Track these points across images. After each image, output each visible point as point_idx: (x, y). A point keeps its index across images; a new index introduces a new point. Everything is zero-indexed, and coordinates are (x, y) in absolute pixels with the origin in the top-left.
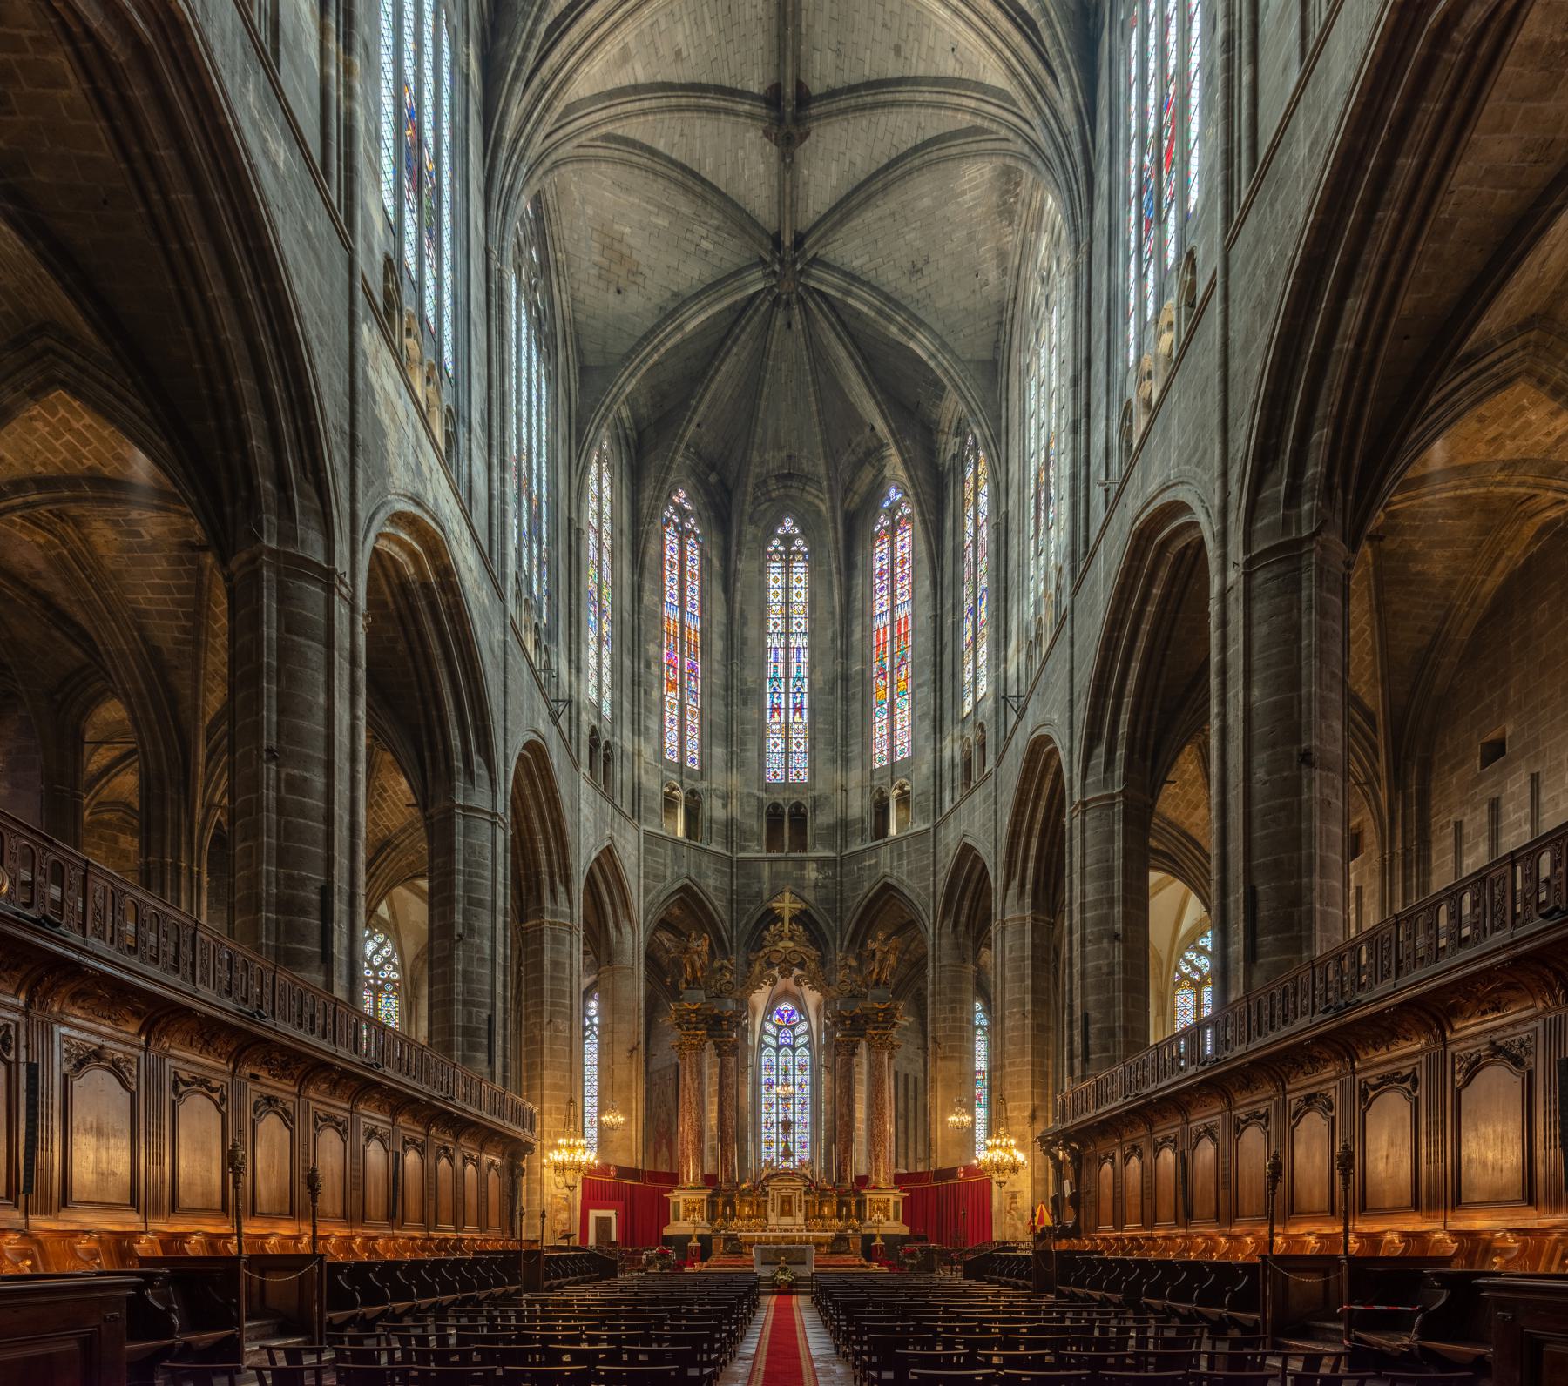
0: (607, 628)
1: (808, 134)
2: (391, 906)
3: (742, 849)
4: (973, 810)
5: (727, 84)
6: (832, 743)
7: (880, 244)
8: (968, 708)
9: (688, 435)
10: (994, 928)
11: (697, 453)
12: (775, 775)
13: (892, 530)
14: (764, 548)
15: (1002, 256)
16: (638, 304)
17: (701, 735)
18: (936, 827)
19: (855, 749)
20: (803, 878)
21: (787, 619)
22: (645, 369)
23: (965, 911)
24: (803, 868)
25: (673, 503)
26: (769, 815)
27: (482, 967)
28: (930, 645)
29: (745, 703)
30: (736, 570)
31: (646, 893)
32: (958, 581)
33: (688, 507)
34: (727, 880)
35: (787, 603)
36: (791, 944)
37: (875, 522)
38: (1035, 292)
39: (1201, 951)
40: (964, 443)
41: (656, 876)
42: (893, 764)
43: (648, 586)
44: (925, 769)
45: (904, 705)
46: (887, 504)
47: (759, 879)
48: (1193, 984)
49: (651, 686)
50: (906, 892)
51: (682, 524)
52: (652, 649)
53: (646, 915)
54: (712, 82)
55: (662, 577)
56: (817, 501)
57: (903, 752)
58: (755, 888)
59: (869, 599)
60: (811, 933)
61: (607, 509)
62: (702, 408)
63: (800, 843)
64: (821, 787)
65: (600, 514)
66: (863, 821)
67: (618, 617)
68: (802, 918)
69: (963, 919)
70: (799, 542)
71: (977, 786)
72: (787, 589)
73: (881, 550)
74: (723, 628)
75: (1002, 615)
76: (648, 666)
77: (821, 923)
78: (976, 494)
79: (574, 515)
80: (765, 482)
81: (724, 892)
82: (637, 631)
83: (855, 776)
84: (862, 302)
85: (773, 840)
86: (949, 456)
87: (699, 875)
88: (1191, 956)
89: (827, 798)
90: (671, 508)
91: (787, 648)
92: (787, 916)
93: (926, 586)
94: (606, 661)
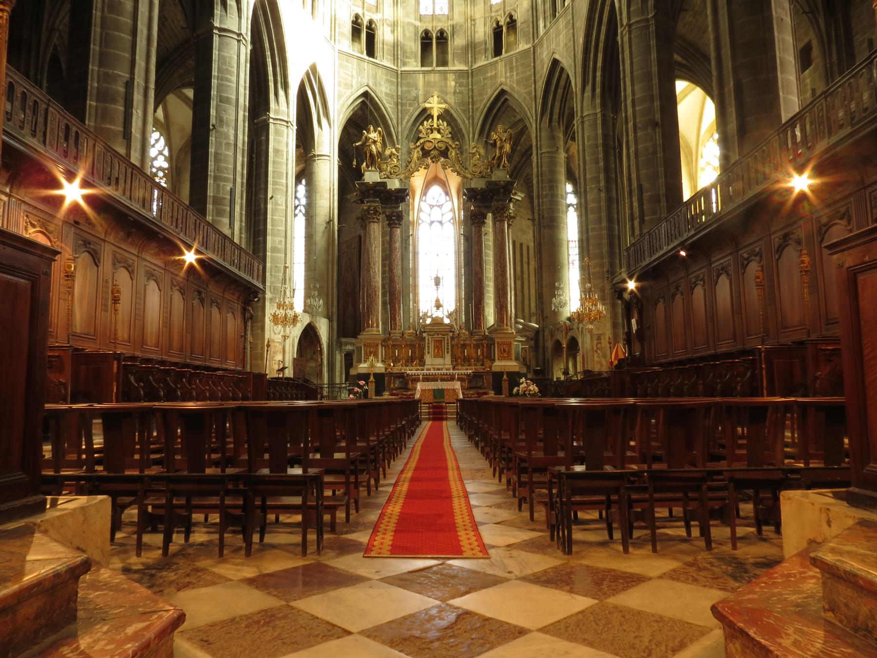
2: (165, 110)
3: (404, 64)
4: (558, 34)
10: (576, 122)
18: (534, 47)
20: (446, 86)
23: (556, 110)
24: (446, 79)
26: (422, 39)
27: (228, 150)
31: (340, 96)
34: (394, 88)
36: (439, 136)
41: (346, 85)
50: (516, 96)
53: (339, 114)
58: (414, 94)
60: (452, 128)
63: (443, 62)
64: (458, 18)
66: (486, 44)
68: (445, 115)
69: (555, 117)
71: (561, 16)
77: (459, 121)
81: (392, 96)
83: (479, 12)
87: (375, 84)
89: (461, 26)
92: (435, 114)
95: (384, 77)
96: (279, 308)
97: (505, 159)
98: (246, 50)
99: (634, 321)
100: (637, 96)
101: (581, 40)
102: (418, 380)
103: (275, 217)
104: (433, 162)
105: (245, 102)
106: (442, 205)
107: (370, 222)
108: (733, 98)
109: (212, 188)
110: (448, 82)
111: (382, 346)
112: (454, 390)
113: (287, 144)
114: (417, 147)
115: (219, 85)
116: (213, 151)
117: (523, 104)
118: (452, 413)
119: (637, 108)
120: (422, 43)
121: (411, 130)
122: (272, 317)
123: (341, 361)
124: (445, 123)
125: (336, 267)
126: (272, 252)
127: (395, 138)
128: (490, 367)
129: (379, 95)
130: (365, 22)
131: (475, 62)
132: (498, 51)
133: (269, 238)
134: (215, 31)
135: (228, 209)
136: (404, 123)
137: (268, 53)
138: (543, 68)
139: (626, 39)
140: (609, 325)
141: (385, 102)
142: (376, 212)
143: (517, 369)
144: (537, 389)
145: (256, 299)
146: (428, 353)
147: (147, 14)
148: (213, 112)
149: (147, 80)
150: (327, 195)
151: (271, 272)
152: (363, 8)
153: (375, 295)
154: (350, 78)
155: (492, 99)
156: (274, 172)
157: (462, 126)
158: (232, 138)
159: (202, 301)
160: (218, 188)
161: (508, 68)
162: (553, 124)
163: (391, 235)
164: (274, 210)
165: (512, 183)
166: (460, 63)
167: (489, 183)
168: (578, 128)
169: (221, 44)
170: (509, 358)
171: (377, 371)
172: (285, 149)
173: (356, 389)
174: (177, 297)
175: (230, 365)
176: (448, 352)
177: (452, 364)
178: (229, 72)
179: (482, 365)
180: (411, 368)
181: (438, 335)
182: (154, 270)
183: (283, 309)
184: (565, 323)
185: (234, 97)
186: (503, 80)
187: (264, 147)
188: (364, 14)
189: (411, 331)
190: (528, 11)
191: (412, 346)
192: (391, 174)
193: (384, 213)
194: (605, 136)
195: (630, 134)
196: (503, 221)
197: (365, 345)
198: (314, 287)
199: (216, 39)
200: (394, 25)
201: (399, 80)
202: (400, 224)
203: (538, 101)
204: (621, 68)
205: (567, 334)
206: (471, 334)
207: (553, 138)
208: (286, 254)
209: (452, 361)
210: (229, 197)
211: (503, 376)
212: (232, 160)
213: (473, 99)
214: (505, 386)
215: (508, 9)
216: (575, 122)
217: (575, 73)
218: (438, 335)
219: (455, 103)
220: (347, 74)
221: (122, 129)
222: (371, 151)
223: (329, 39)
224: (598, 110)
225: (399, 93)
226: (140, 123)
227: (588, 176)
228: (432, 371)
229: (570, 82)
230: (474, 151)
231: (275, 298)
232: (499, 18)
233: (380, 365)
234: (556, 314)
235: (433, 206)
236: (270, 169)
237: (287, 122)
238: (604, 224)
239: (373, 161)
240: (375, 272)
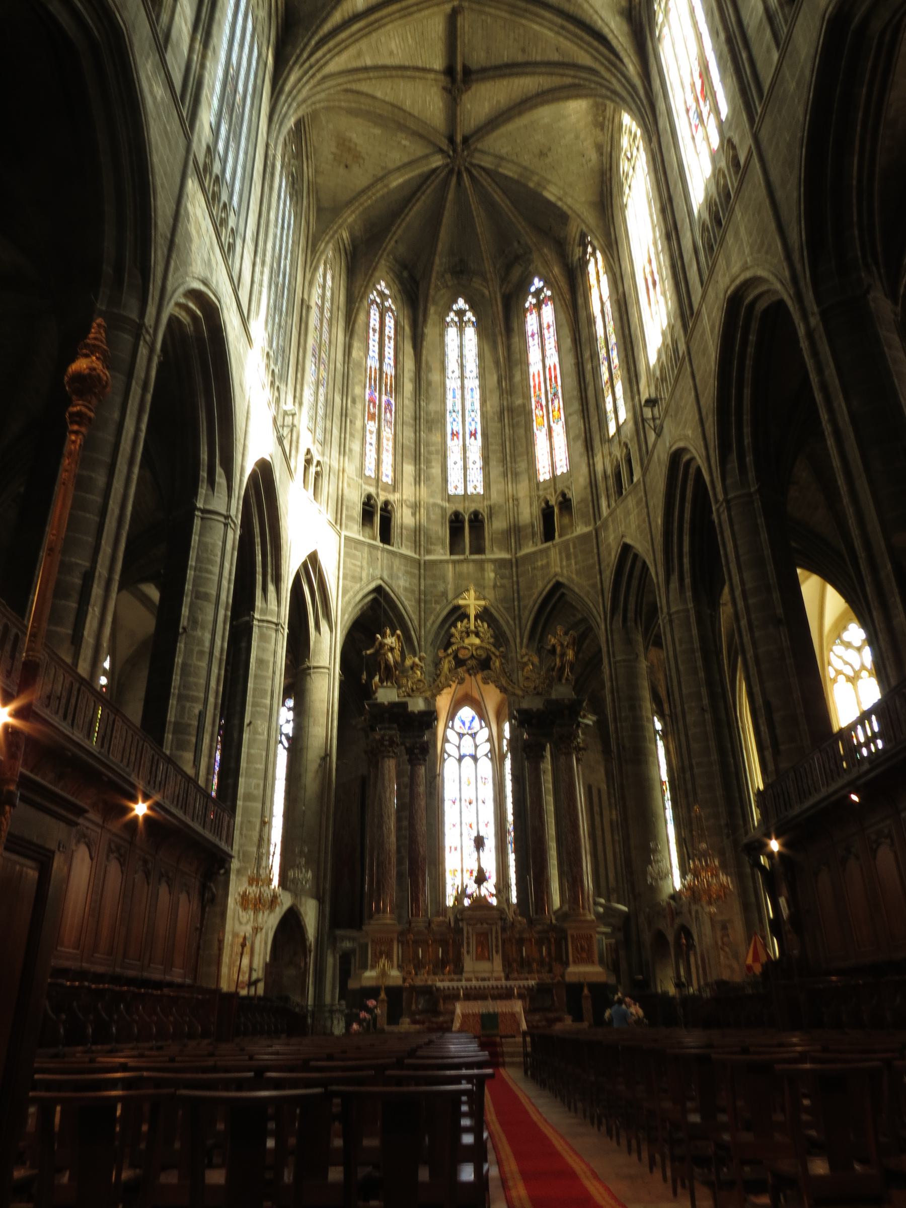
0: (323, 374)
1: (470, 88)
3: (428, 552)
5: (420, 64)
6: (503, 461)
7: (518, 141)
8: (612, 430)
9: (389, 247)
11: (396, 260)
12: (456, 487)
13: (538, 306)
14: (443, 320)
15: (599, 148)
16: (360, 178)
17: (395, 455)
19: (522, 466)
20: (484, 579)
21: (462, 367)
22: (361, 208)
24: (482, 569)
25: (377, 290)
26: (451, 522)
28: (575, 384)
29: (430, 430)
30: (423, 335)
31: (344, 594)
32: (593, 338)
33: (387, 292)
34: (416, 581)
35: (461, 356)
37: (525, 300)
38: (624, 166)
39: (848, 645)
40: (585, 252)
41: (353, 577)
42: (554, 477)
43: (356, 344)
44: (582, 479)
45: (559, 430)
46: (533, 289)
47: (444, 578)
48: (849, 679)
49: (355, 417)
50: (576, 590)
51: (383, 303)
52: (358, 390)
53: (343, 614)
54: (411, 64)
55: (368, 338)
56: (481, 288)
57: (562, 467)
58: (441, 588)
59: (525, 351)
61: (328, 294)
62: (400, 232)
63: (478, 549)
64: (496, 497)
65: (323, 297)
66: (533, 526)
67: (332, 366)
69: (631, 615)
70: (469, 315)
72: (461, 347)
73: (531, 322)
74: (412, 374)
75: (631, 361)
76: (354, 402)
78: (599, 281)
79: (306, 297)
80: (443, 276)
81: (413, 592)
82: (346, 377)
83: (523, 489)
84: (508, 171)
85: (455, 545)
86: (577, 257)
87: (391, 576)
88: (838, 649)
89: (500, 507)
90: (375, 293)
91: (463, 387)
93: (568, 342)
94: (322, 398)
95: (402, 568)
96: (251, 884)
97: (567, 670)
98: (233, 536)
99: (782, 901)
100: (749, 586)
101: (660, 521)
102: (456, 997)
103: (252, 751)
104: (470, 675)
105: (227, 597)
106: (475, 734)
107: (383, 757)
108: (894, 584)
109: (174, 711)
110: (486, 574)
111: (398, 941)
112: (513, 1015)
113: (275, 653)
114: (448, 655)
115: (196, 578)
116: (180, 661)
117: (586, 599)
118: (512, 1055)
119: (751, 601)
120: (451, 528)
121: (437, 634)
122: (239, 899)
123: (335, 965)
124: (486, 625)
125: (331, 822)
126: (245, 800)
127: (416, 643)
128: (563, 976)
129: (396, 589)
130: (379, 504)
131: (520, 549)
132: (549, 535)
133: (242, 780)
134: (198, 513)
135: (194, 739)
136: (429, 624)
137: (258, 540)
138: (610, 554)
139: (725, 516)
140: (736, 906)
141: (403, 599)
142: (392, 743)
143: (603, 978)
144: (641, 1012)
145: (222, 871)
146: (468, 952)
147: (122, 490)
148: (185, 611)
149: (111, 570)
150: (323, 721)
151: (241, 829)
152: (377, 487)
153: (390, 863)
154: (359, 570)
155: (544, 593)
156: (255, 690)
157: (505, 628)
158: (207, 644)
159: (147, 874)
160: (182, 711)
161: (564, 556)
162: (629, 624)
163: (413, 777)
164: (252, 742)
165: (580, 702)
166: (501, 550)
167: (549, 702)
168: (664, 627)
169: (203, 528)
170: (589, 961)
171: (391, 983)
172: (272, 659)
173: (363, 1014)
174: (114, 868)
175: (177, 975)
176: (497, 952)
177: (504, 971)
178: (211, 562)
179: (550, 971)
180: (442, 977)
181: (482, 924)
182: (87, 828)
183: (257, 885)
184: (669, 904)
185: (214, 592)
186: (558, 570)
187: (243, 657)
188: (378, 495)
189: (441, 918)
190: (585, 488)
191: (443, 943)
192: (413, 690)
193: (403, 744)
194: (703, 638)
195: (744, 633)
196: (569, 755)
197: (373, 941)
198: (301, 852)
199: (197, 523)
200: (416, 507)
201: (422, 571)
202: (425, 760)
203: (606, 594)
204: (722, 552)
205: (673, 920)
206: (531, 922)
207: (629, 642)
208: (264, 803)
209: (504, 966)
210: (195, 723)
211: (582, 990)
212: (204, 673)
213: (518, 593)
214: (587, 1005)
215: (560, 487)
216: (660, 621)
217: (655, 560)
218: (482, 924)
219: (496, 599)
220: (355, 565)
221: (70, 632)
222: (387, 661)
223: (334, 523)
224: (691, 605)
225: (422, 588)
226: (95, 624)
227: (685, 691)
228: (474, 983)
229: (648, 569)
230: (525, 659)
231: (246, 869)
232: (548, 497)
233: (395, 973)
234: (653, 890)
235: (463, 735)
236: (250, 685)
237: (277, 625)
238: (714, 757)
239: (389, 674)
240: (390, 828)
